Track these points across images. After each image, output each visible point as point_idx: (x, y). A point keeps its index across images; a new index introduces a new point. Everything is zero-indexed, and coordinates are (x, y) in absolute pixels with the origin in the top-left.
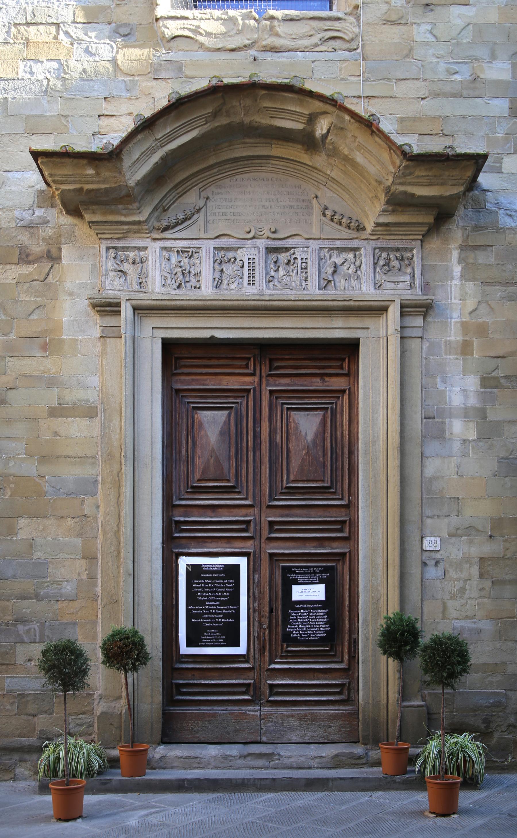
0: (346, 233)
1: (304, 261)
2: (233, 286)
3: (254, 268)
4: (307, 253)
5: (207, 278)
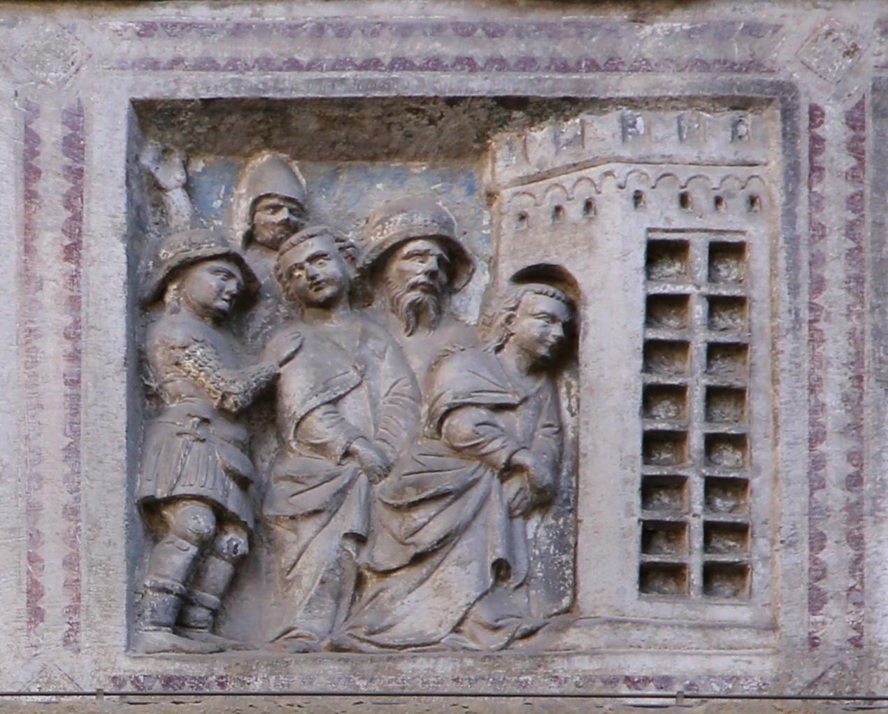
2: (420, 608)
3: (727, 373)
5: (53, 497)
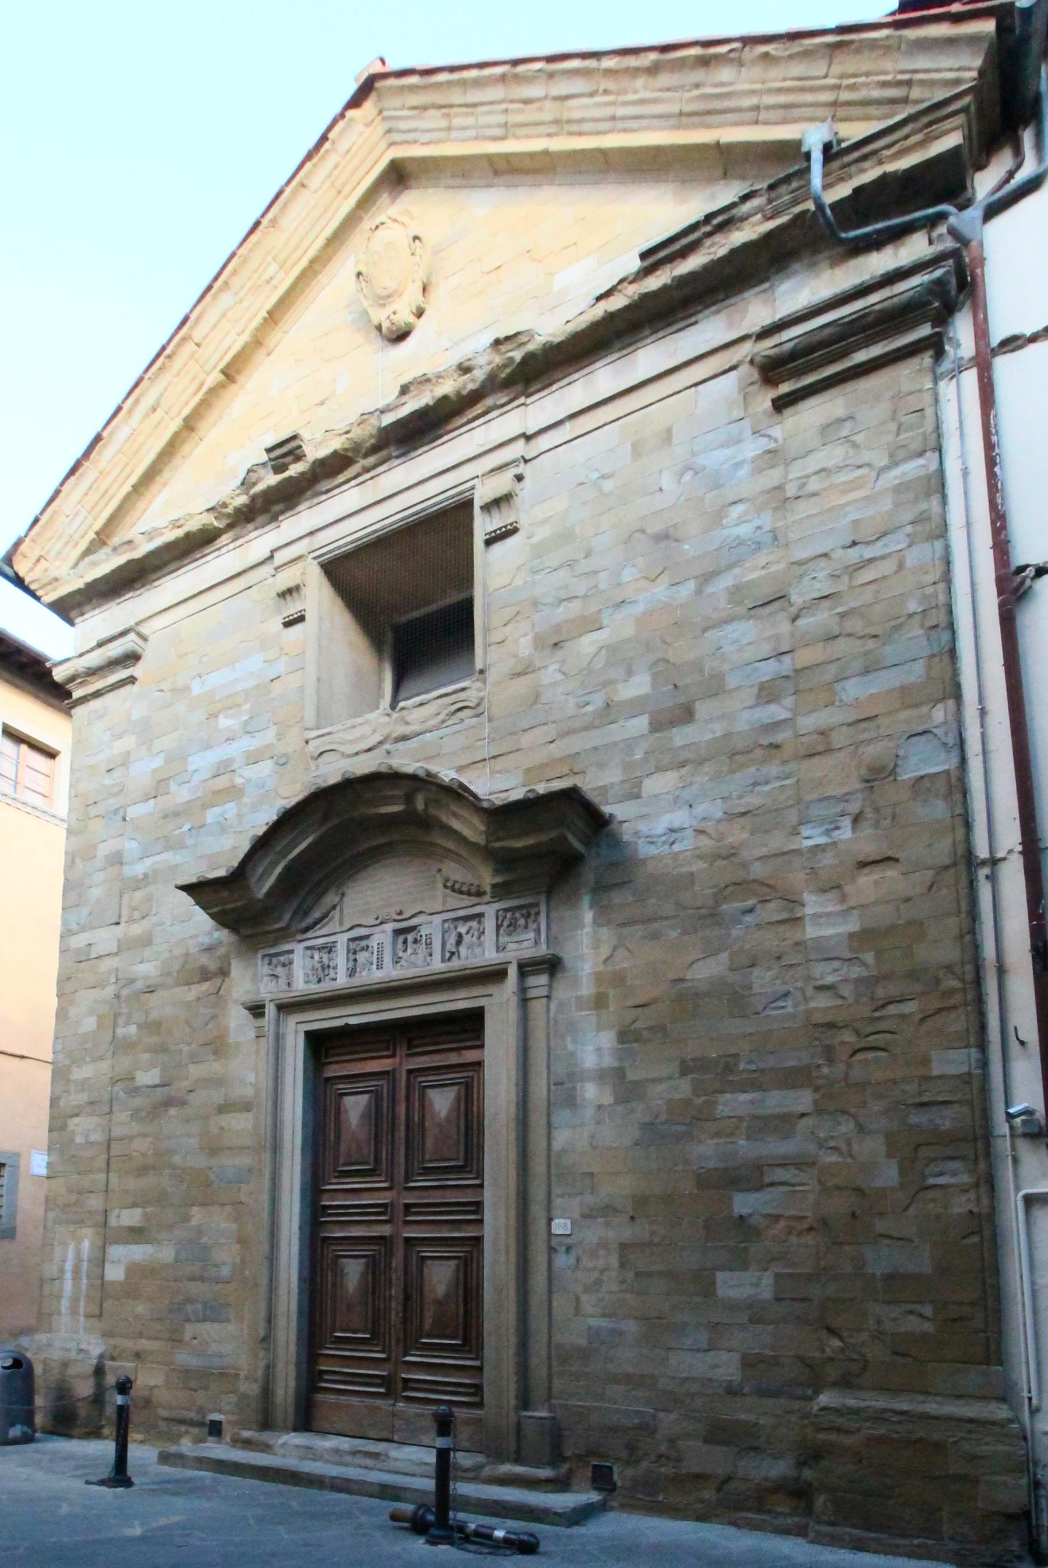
0: (468, 901)
1: (429, 937)
4: (432, 927)
